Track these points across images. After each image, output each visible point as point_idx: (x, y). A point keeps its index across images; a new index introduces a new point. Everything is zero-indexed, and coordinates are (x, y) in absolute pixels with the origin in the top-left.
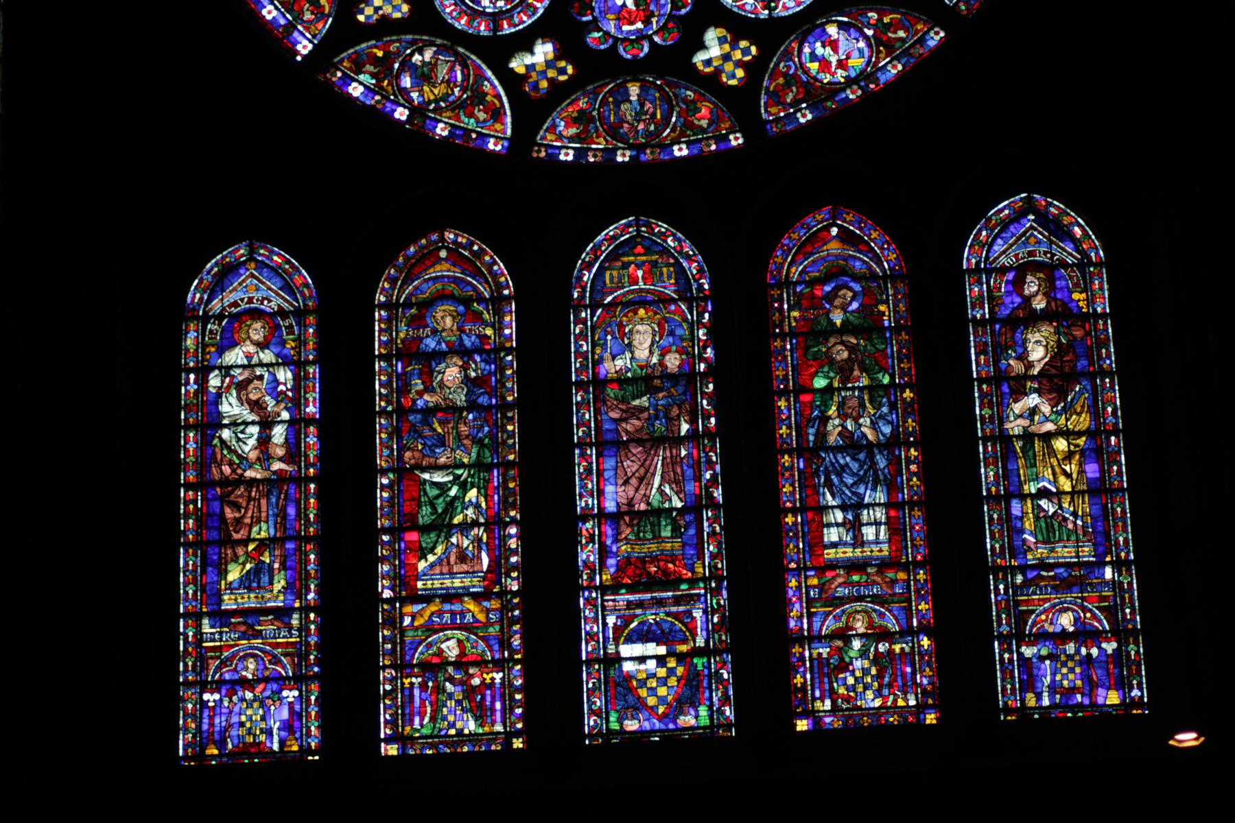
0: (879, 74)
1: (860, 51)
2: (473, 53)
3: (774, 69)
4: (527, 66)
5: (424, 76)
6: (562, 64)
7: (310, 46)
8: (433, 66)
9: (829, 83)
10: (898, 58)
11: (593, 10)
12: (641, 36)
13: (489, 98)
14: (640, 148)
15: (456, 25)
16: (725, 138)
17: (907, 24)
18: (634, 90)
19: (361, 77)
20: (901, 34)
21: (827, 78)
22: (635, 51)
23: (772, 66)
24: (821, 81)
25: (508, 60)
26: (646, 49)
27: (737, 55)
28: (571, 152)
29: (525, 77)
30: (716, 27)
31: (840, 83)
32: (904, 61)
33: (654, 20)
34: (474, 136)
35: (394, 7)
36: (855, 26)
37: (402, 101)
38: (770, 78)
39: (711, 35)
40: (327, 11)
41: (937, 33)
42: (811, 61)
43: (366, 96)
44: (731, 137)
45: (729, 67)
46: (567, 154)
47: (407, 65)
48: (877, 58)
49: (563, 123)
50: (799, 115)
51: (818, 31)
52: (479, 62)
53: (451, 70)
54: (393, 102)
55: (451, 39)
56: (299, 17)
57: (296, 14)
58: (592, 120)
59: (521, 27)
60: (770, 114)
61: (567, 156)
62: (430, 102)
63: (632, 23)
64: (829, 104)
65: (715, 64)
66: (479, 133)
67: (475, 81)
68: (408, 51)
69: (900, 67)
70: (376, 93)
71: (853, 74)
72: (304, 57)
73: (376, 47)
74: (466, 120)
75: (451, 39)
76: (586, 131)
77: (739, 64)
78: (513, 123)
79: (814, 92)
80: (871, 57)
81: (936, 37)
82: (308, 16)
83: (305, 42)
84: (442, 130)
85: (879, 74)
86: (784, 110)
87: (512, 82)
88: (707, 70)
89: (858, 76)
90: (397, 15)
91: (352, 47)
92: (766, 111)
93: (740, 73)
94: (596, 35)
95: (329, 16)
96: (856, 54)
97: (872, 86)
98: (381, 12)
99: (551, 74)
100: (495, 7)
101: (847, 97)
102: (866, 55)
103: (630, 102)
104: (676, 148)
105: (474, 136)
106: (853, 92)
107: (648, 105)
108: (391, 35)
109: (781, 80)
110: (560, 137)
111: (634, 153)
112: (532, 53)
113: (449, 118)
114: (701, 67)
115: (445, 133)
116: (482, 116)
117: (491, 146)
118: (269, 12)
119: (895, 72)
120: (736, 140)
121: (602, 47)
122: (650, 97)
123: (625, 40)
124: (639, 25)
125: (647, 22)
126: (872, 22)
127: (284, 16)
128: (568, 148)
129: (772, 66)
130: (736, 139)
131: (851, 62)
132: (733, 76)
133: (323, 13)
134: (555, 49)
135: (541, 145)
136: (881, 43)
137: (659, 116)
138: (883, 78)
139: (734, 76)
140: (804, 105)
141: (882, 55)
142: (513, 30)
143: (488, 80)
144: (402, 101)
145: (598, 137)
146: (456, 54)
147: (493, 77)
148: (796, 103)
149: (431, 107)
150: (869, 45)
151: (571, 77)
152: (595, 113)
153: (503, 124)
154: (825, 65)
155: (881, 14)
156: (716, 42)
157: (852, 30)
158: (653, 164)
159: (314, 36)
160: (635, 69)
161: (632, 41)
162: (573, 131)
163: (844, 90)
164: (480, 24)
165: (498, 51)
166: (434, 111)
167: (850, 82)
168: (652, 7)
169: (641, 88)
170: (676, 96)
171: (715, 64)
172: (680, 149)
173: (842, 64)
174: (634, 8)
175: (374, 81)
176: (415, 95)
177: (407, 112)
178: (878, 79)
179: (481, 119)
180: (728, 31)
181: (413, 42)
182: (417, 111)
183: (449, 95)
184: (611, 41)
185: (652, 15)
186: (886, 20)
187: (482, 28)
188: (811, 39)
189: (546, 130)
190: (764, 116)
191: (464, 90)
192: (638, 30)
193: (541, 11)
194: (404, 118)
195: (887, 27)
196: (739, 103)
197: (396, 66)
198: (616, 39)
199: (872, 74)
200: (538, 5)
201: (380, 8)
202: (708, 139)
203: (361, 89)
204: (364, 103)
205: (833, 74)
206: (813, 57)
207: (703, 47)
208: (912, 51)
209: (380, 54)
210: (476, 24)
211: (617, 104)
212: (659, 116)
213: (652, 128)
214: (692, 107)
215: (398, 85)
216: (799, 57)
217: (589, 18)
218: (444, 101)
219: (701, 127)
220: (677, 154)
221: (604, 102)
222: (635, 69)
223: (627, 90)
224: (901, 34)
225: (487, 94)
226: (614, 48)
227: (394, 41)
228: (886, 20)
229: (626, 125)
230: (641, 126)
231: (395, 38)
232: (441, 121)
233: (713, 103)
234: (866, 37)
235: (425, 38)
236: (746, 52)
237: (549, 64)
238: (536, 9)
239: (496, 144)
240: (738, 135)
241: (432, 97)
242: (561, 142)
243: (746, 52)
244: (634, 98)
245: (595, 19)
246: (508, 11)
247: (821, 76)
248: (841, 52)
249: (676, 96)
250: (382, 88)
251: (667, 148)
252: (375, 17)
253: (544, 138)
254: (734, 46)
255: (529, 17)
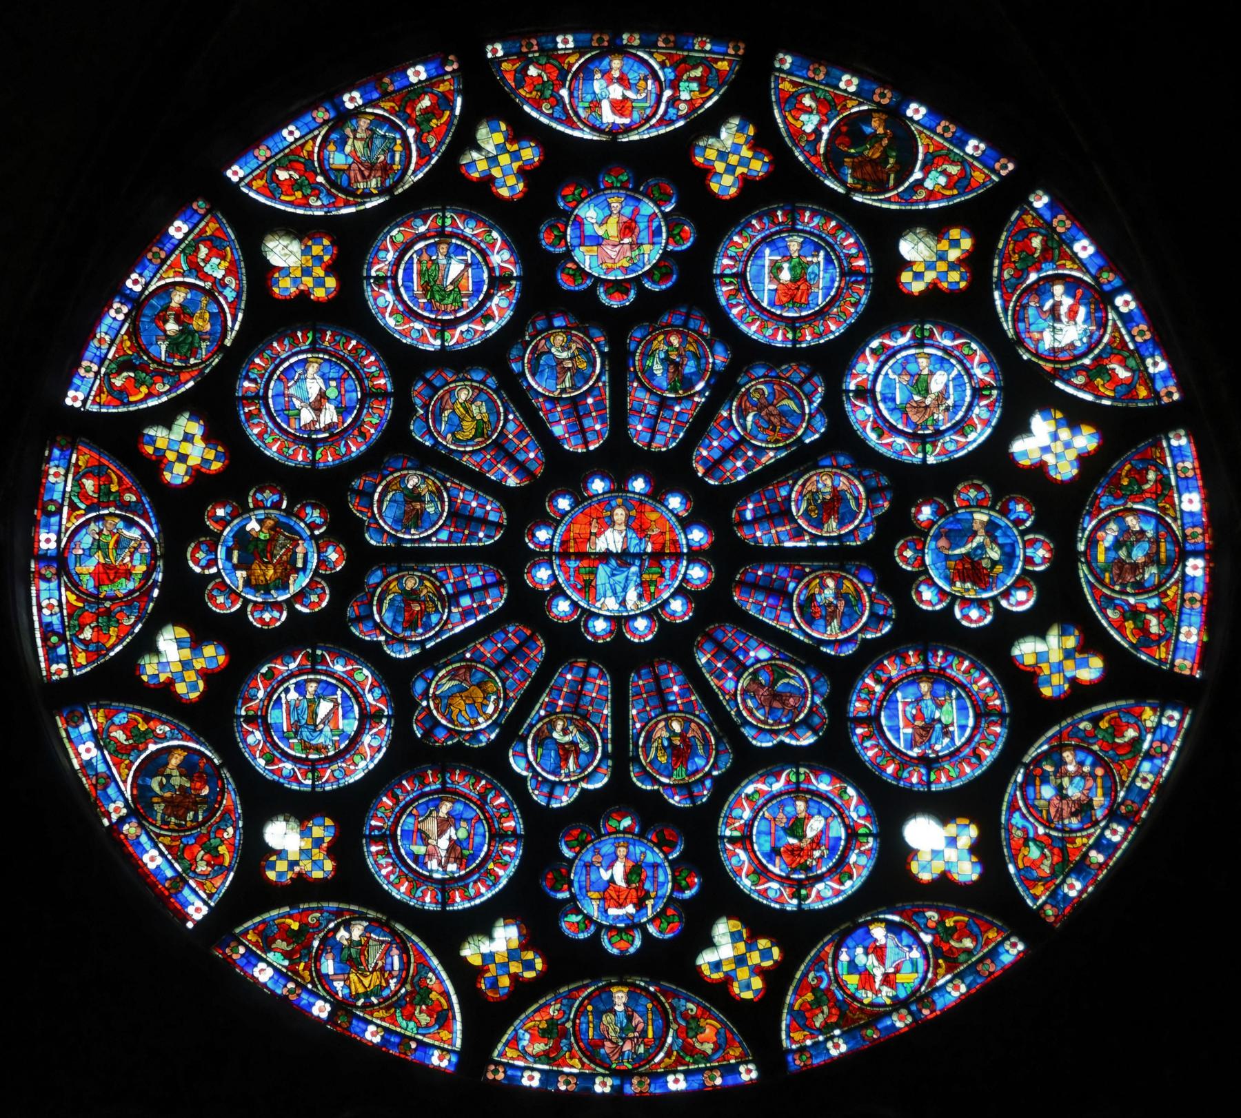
0: (936, 996)
1: (914, 963)
2: (414, 932)
3: (801, 980)
4: (483, 955)
5: (352, 961)
6: (529, 955)
7: (205, 910)
8: (363, 946)
9: (872, 1004)
10: (961, 976)
11: (571, 884)
12: (633, 925)
13: (434, 996)
14: (625, 1075)
15: (394, 893)
16: (732, 1070)
17: (976, 930)
18: (620, 997)
19: (271, 956)
20: (968, 943)
21: (867, 997)
22: (623, 945)
23: (798, 975)
24: (860, 1001)
25: (459, 947)
26: (638, 943)
27: (754, 958)
28: (537, 1076)
29: (480, 971)
30: (729, 918)
31: (885, 1005)
32: (969, 979)
33: (649, 903)
34: (413, 1045)
35: (314, 862)
36: (909, 929)
37: (322, 993)
38: (795, 993)
39: (722, 929)
40: (226, 864)
41: (1014, 945)
42: (850, 973)
43: (276, 982)
44: (742, 1069)
45: (743, 973)
46: (531, 1078)
47: (328, 942)
48: (935, 974)
49: (527, 1036)
50: (830, 1045)
51: (860, 932)
52: (422, 945)
53: (387, 953)
54: (311, 993)
55: (392, 914)
56: (191, 868)
57: (187, 864)
58: (564, 1034)
59: (478, 901)
60: (793, 1041)
61: (531, 1081)
62: (358, 996)
63: (621, 906)
64: (869, 1032)
65: (726, 968)
66: (419, 1042)
67: (417, 972)
68: (332, 925)
69: (963, 989)
70: (289, 979)
71: (902, 994)
72: (198, 924)
73: (290, 916)
74: (404, 1024)
75: (392, 914)
76: (556, 1048)
77: (757, 970)
78: (464, 1032)
79: (851, 1016)
80: (926, 972)
81: (1012, 951)
82: (202, 867)
83: (199, 904)
84: (373, 1034)
85: (936, 996)
86: (812, 1036)
87: (465, 976)
88: (715, 976)
89: (909, 997)
90: (318, 874)
91: (259, 914)
92: (788, 1036)
93: (757, 983)
94: (574, 918)
95: (229, 869)
96: (907, 967)
97: (926, 1012)
98: (297, 869)
99: (515, 968)
100: (445, 871)
101: (893, 1025)
102: (921, 967)
103: (615, 1013)
104: (670, 1078)
105: (413, 1045)
106: (901, 1019)
107: (637, 1019)
108: (309, 901)
109: (809, 997)
110: (524, 1054)
111: (617, 1082)
112: (491, 938)
113: (382, 1019)
114: (706, 971)
115: (377, 1039)
116: (424, 1019)
117: (435, 1061)
118: (152, 859)
119: (956, 994)
120: (748, 1074)
121: (581, 936)
122: (640, 1009)
123: (611, 928)
124: (630, 909)
125: (640, 905)
126: (931, 924)
127: (172, 866)
128: (533, 1069)
129: (798, 975)
130: (748, 1071)
131: (900, 978)
132: (748, 987)
133: (221, 865)
134: (520, 934)
135: (498, 1063)
136: (941, 955)
137: (650, 1035)
138: (941, 1002)
139: (748, 987)
140: (837, 1032)
141: (941, 971)
142: (467, 905)
143: (433, 971)
144: (322, 993)
145: (571, 1058)
146: (394, 933)
147: (440, 968)
148: (827, 1028)
149: (360, 1003)
150: (926, 957)
151: (541, 976)
152: (569, 1025)
153: (451, 1032)
154: (867, 978)
155: (944, 914)
156: (728, 939)
157: (904, 934)
158: (643, 1100)
159: (210, 896)
160: (622, 969)
161: (619, 931)
162: (539, 1047)
163: (889, 1014)
164: (424, 894)
165: (447, 931)
166: (364, 1007)
167: (898, 1004)
168: (648, 886)
169: (629, 994)
170: (674, 1009)
171: (726, 968)
172: (676, 1081)
173: (888, 980)
174: (624, 885)
175: (286, 963)
176: (338, 985)
177: (328, 1007)
178: (934, 1002)
179: (423, 1023)
180: (745, 924)
181: (338, 913)
182: (341, 1007)
183: (383, 988)
184: (592, 928)
185: (647, 895)
186: (949, 923)
187: (428, 899)
188: (850, 943)
189: (506, 1044)
190: (786, 1043)
191: (402, 983)
192: (629, 916)
193: (504, 881)
194: (324, 1015)
195: (950, 932)
196: (755, 1023)
197: (316, 943)
198: (600, 927)
199: (927, 995)
200: (501, 872)
201: (296, 863)
202: (712, 1069)
203: (270, 972)
204: (273, 992)
205: (878, 992)
206: (853, 967)
207: (710, 943)
208: (979, 967)
209: (295, 926)
210: (419, 894)
211: (598, 1015)
212: (650, 1035)
213: (641, 1050)
214: (693, 1025)
215: (318, 971)
216: (834, 966)
217: (566, 895)
218: (376, 996)
219: (704, 1052)
220: (672, 1086)
221: (581, 1011)
222: (622, 969)
223: (611, 996)
224: (968, 943)
225: (430, 990)
226: (596, 938)
227: (313, 910)
228: (949, 923)
229: (608, 1044)
230: (627, 1047)
231: (314, 905)
232: (371, 1023)
233: (720, 1022)
234: (922, 945)
235: (353, 907)
236: (766, 954)
237: (512, 955)
238: (498, 878)
239: (441, 1059)
240: (751, 1066)
241: (361, 990)
242: (523, 1059)
243: (766, 954)
244: (619, 1008)
245: (573, 898)
246: (461, 878)
247: (861, 994)
248: (888, 963)
249: (674, 1009)
250: (296, 973)
251: (658, 1077)
252: (290, 875)
253: (502, 1054)
254: (751, 946)
255: (489, 888)
